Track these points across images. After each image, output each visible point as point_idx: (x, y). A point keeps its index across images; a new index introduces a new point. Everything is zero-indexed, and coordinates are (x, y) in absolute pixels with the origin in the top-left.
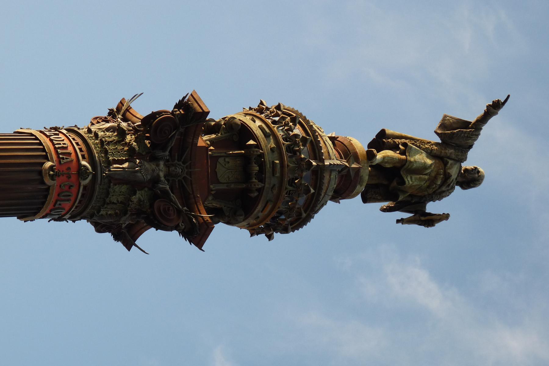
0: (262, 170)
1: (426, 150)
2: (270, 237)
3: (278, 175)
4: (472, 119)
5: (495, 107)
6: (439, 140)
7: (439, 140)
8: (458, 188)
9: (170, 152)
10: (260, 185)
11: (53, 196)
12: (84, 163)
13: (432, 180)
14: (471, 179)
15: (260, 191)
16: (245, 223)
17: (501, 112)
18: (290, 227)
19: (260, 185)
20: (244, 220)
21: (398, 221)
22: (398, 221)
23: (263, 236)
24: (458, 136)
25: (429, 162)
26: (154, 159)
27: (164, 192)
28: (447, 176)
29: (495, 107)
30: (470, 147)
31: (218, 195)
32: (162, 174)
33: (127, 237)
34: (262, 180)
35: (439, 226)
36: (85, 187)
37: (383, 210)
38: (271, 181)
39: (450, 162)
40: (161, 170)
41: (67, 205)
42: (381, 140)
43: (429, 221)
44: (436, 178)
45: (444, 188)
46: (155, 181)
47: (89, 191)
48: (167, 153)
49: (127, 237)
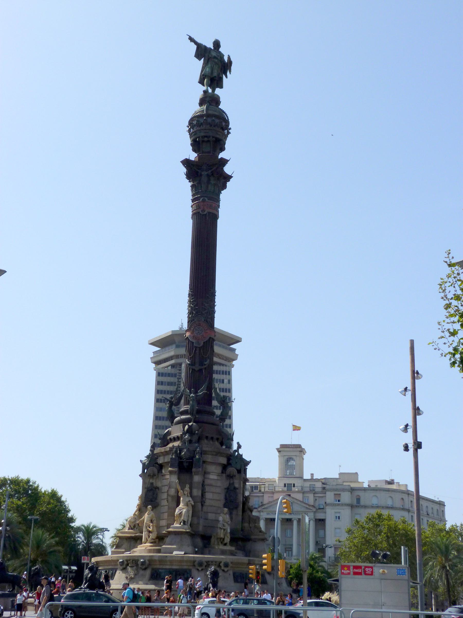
0: (206, 137)
1: (205, 66)
2: (230, 129)
3: (208, 131)
4: (196, 46)
5: (191, 39)
6: (203, 59)
7: (203, 59)
8: (220, 50)
9: (199, 169)
10: (211, 137)
11: (211, 211)
12: (201, 200)
13: (216, 63)
14: (217, 44)
15: (213, 137)
16: (224, 140)
17: (192, 37)
18: (227, 124)
19: (211, 137)
20: (223, 141)
21: (230, 74)
22: (230, 74)
23: (230, 131)
24: (201, 52)
25: (209, 65)
26: (201, 175)
27: (212, 172)
28: (215, 57)
29: (191, 39)
30: (205, 47)
31: (215, 150)
32: (206, 173)
33: (228, 178)
34: (210, 137)
35: (232, 59)
36: (209, 200)
37: (226, 77)
38: (210, 134)
39: (210, 56)
40: (204, 173)
41: (214, 205)
42: (201, 82)
43: (230, 62)
44: (215, 62)
45: (219, 58)
46: (208, 175)
47: (210, 199)
48: (199, 171)
49: (228, 178)
